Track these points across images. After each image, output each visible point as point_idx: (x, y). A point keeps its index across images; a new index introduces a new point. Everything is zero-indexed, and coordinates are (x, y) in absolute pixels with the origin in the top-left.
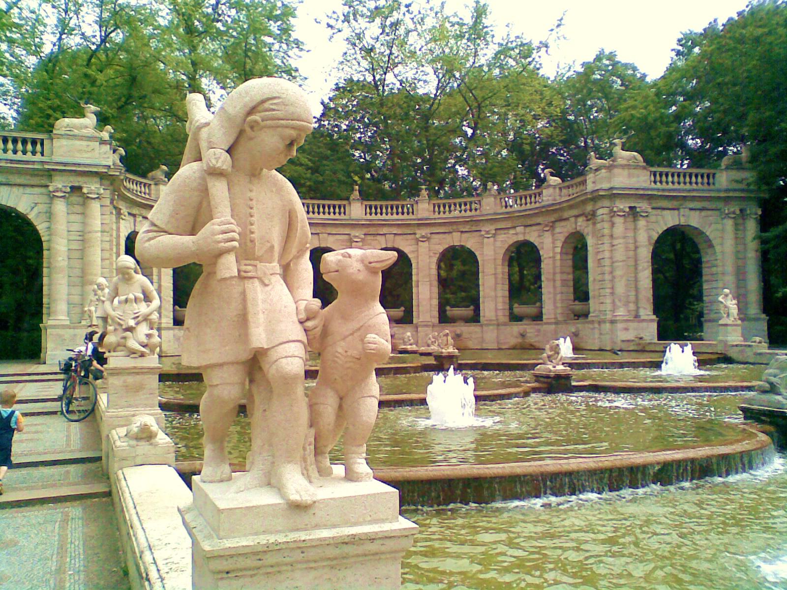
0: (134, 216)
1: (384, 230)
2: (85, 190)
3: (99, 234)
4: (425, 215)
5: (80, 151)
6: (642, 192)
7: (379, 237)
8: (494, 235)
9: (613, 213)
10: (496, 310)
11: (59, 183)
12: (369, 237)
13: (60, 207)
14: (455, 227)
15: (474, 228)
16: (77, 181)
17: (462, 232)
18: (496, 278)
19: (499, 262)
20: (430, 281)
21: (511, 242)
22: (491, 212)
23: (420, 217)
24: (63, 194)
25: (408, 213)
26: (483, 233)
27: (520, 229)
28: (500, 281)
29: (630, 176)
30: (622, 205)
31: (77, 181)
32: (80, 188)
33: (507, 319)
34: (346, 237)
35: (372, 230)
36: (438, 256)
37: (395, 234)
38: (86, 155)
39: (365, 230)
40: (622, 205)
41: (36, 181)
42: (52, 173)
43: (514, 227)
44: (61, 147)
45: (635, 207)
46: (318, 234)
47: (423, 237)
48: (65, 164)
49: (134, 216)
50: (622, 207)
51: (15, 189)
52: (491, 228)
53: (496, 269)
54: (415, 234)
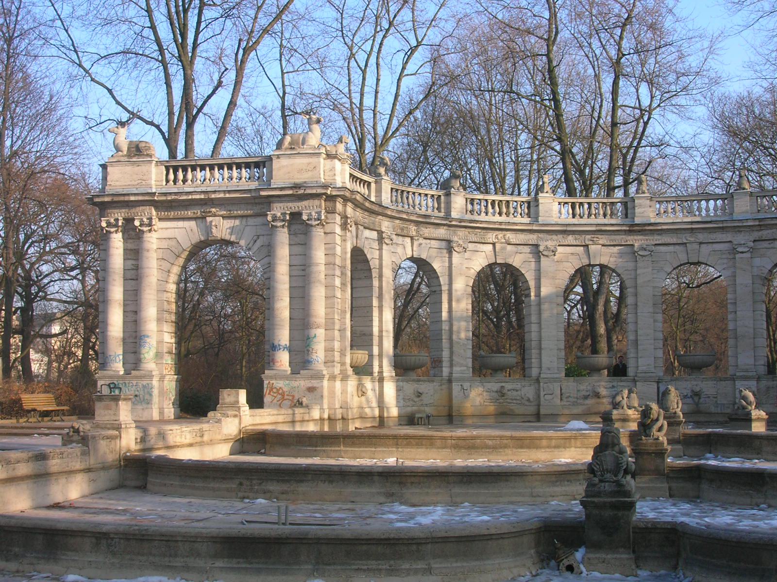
2: (305, 217)
5: (300, 171)
12: (765, 244)
24: (282, 224)
31: (295, 206)
32: (299, 214)
35: (766, 233)
39: (756, 235)
42: (272, 199)
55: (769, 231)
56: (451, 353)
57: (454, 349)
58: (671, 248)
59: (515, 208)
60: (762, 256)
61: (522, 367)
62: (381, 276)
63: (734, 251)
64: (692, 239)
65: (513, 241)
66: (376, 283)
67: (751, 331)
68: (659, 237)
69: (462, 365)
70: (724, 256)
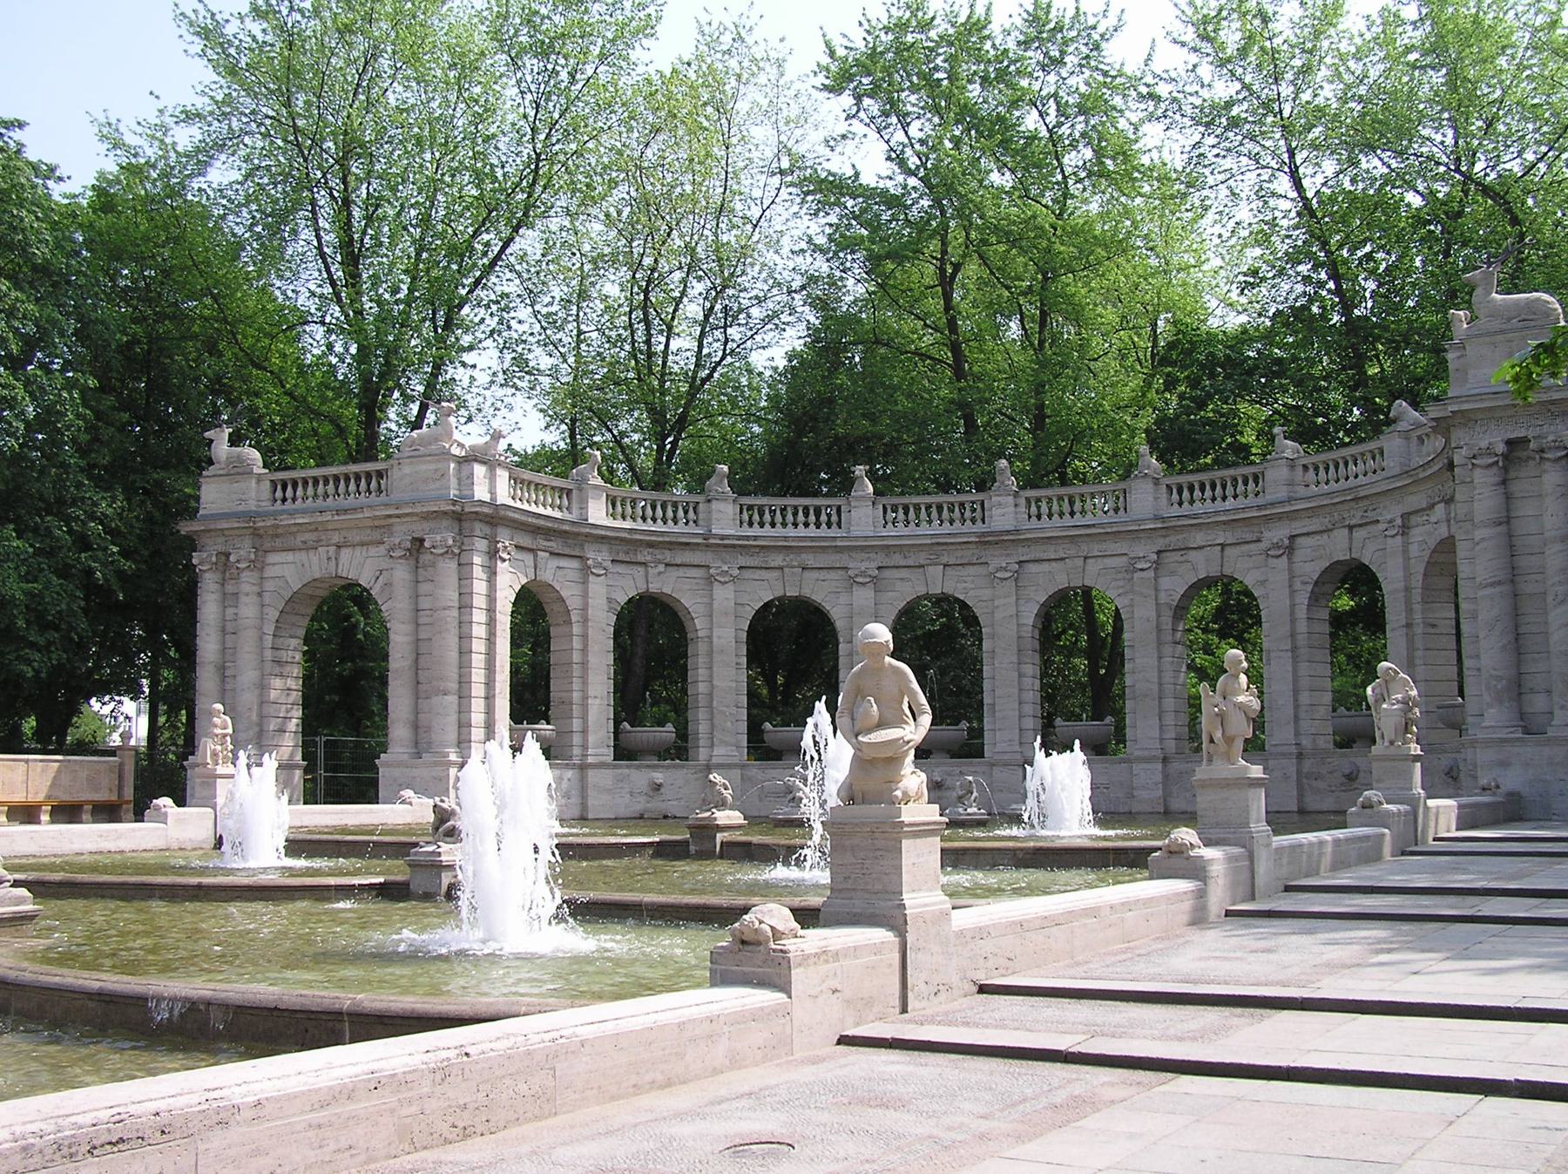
0: (644, 564)
1: (1199, 538)
2: (427, 544)
3: (455, 613)
4: (1282, 493)
5: (426, 481)
7: (1192, 555)
8: (1405, 529)
12: (1176, 556)
13: (401, 573)
16: (419, 529)
17: (1351, 528)
20: (1294, 649)
21: (1432, 543)
22: (1397, 471)
23: (1269, 498)
25: (829, 525)
26: (1382, 526)
27: (1440, 508)
33: (608, 754)
34: (1121, 562)
35: (1174, 540)
36: (1310, 588)
37: (1223, 546)
43: (1432, 506)
45: (1524, 441)
46: (1062, 559)
47: (1277, 546)
49: (644, 564)
50: (1484, 444)
52: (1392, 511)
54: (1259, 541)
55: (1180, 537)
56: (713, 726)
57: (716, 721)
58: (1045, 567)
59: (829, 515)
60: (1173, 573)
61: (679, 750)
62: (585, 621)
63: (1131, 569)
64: (1072, 552)
65: (811, 563)
66: (576, 629)
67: (1155, 688)
68: (1026, 550)
69: (727, 744)
70: (1120, 576)
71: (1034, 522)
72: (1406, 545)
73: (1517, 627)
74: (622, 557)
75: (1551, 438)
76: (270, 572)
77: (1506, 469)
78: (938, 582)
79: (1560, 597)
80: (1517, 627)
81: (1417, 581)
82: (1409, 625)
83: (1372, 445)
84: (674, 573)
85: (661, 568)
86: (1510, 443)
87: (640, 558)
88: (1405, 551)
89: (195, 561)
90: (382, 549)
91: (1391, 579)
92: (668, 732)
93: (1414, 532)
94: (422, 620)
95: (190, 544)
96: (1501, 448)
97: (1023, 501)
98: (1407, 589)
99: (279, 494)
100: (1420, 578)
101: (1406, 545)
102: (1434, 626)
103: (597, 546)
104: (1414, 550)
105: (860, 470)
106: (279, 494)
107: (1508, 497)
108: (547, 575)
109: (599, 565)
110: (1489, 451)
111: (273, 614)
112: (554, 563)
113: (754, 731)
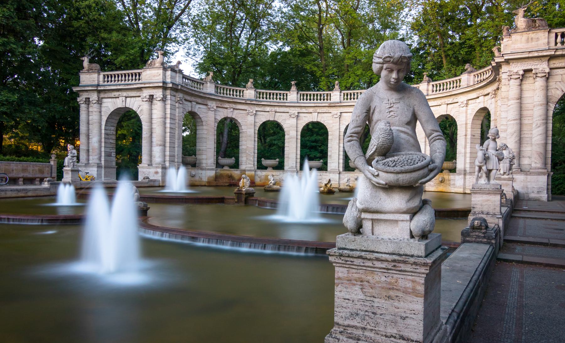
0: (227, 108)
5: (154, 76)
6: (536, 54)
9: (510, 77)
10: (465, 164)
11: (146, 93)
14: (443, 100)
15: (455, 101)
17: (448, 104)
18: (466, 139)
19: (469, 126)
27: (481, 98)
28: (469, 141)
29: (528, 41)
30: (518, 68)
38: (156, 78)
40: (518, 68)
41: (137, 94)
44: (146, 75)
45: (531, 70)
48: (145, 83)
49: (227, 108)
50: (515, 71)
51: (132, 98)
52: (462, 99)
53: (466, 131)
65: (278, 111)
71: (345, 101)
72: (467, 110)
73: (521, 135)
74: (220, 105)
75: (541, 69)
76: (104, 105)
77: (522, 80)
78: (314, 118)
79: (538, 125)
80: (521, 135)
81: (470, 122)
82: (466, 135)
83: (457, 78)
84: (236, 111)
85: (232, 110)
86: (526, 71)
87: (225, 106)
88: (466, 112)
89: (78, 100)
90: (140, 98)
91: (460, 121)
92: (232, 161)
93: (469, 106)
94: (153, 122)
95: (77, 94)
96: (521, 72)
97: (342, 94)
98: (466, 124)
99: (106, 79)
100: (471, 120)
101: (467, 110)
102: (474, 136)
103: (211, 102)
104: (469, 112)
105: (293, 83)
106: (106, 79)
107: (521, 90)
108: (196, 110)
109: (213, 108)
110: (517, 73)
111: (104, 119)
112: (198, 106)
113: (259, 161)
